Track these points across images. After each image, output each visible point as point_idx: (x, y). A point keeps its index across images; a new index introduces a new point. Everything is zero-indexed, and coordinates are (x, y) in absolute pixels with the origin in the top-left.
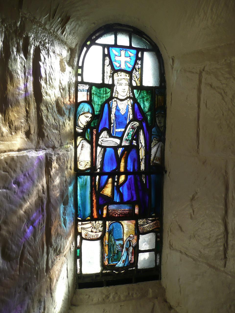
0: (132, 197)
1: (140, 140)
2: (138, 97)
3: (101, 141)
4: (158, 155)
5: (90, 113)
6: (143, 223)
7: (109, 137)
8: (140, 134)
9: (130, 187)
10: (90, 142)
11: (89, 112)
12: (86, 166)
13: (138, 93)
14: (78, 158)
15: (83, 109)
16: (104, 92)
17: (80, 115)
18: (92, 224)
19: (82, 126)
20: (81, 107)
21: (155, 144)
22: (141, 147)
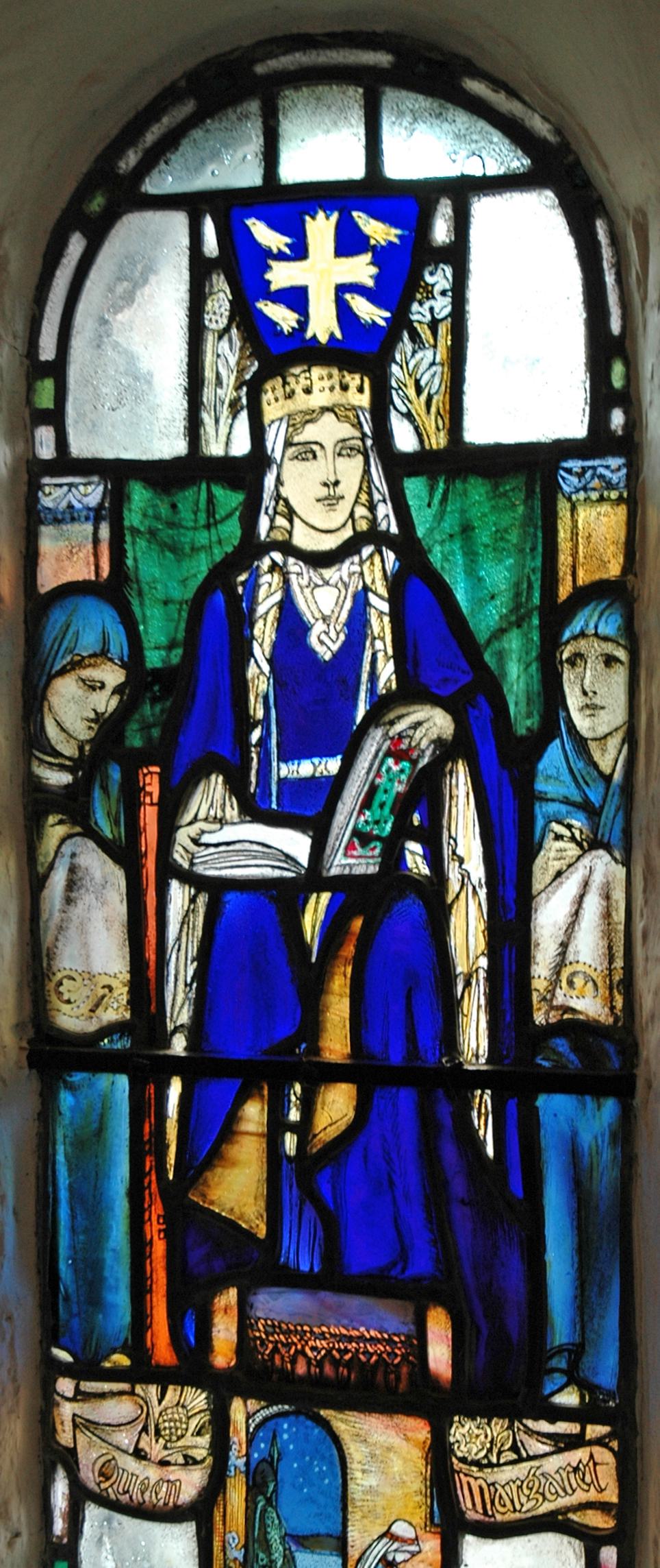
0: (404, 1256)
1: (450, 837)
2: (431, 531)
3: (192, 847)
4: (588, 948)
5: (111, 660)
6: (490, 1450)
7: (240, 813)
8: (454, 792)
9: (389, 1175)
10: (125, 853)
11: (103, 654)
12: (100, 1011)
13: (431, 496)
14: (48, 955)
15: (68, 637)
16: (195, 513)
17: (51, 678)
18: (142, 1402)
19: (69, 750)
20: (58, 625)
21: (557, 865)
22: (457, 888)
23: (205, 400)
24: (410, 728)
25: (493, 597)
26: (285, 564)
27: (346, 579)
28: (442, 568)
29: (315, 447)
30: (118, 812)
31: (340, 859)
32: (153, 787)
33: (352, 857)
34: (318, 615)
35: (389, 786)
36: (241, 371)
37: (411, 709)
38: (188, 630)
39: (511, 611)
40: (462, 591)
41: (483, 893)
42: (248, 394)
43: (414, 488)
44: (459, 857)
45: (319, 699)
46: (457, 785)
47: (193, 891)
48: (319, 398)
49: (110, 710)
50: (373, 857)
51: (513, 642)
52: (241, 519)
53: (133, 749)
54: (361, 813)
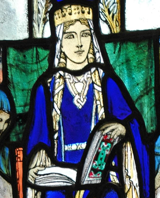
1: (126, 169)
2: (115, 62)
3: (35, 176)
5: (4, 111)
7: (51, 163)
8: (127, 153)
13: (115, 49)
16: (32, 58)
22: (129, 187)
23: (34, 18)
24: (110, 131)
25: (138, 84)
26: (64, 75)
27: (86, 80)
28: (120, 75)
29: (73, 34)
30: (8, 165)
31: (87, 178)
32: (21, 155)
33: (91, 177)
34: (76, 93)
35: (103, 152)
36: (47, 8)
37: (110, 125)
38: (31, 99)
39: (144, 89)
40: (127, 83)
41: (138, 189)
42: (49, 16)
43: (109, 47)
44: (129, 176)
45: (78, 122)
46: (127, 151)
47: (36, 191)
48: (74, 17)
49: (5, 128)
50: (99, 177)
51: (145, 100)
52: (48, 60)
53: (13, 142)
54: (94, 162)
